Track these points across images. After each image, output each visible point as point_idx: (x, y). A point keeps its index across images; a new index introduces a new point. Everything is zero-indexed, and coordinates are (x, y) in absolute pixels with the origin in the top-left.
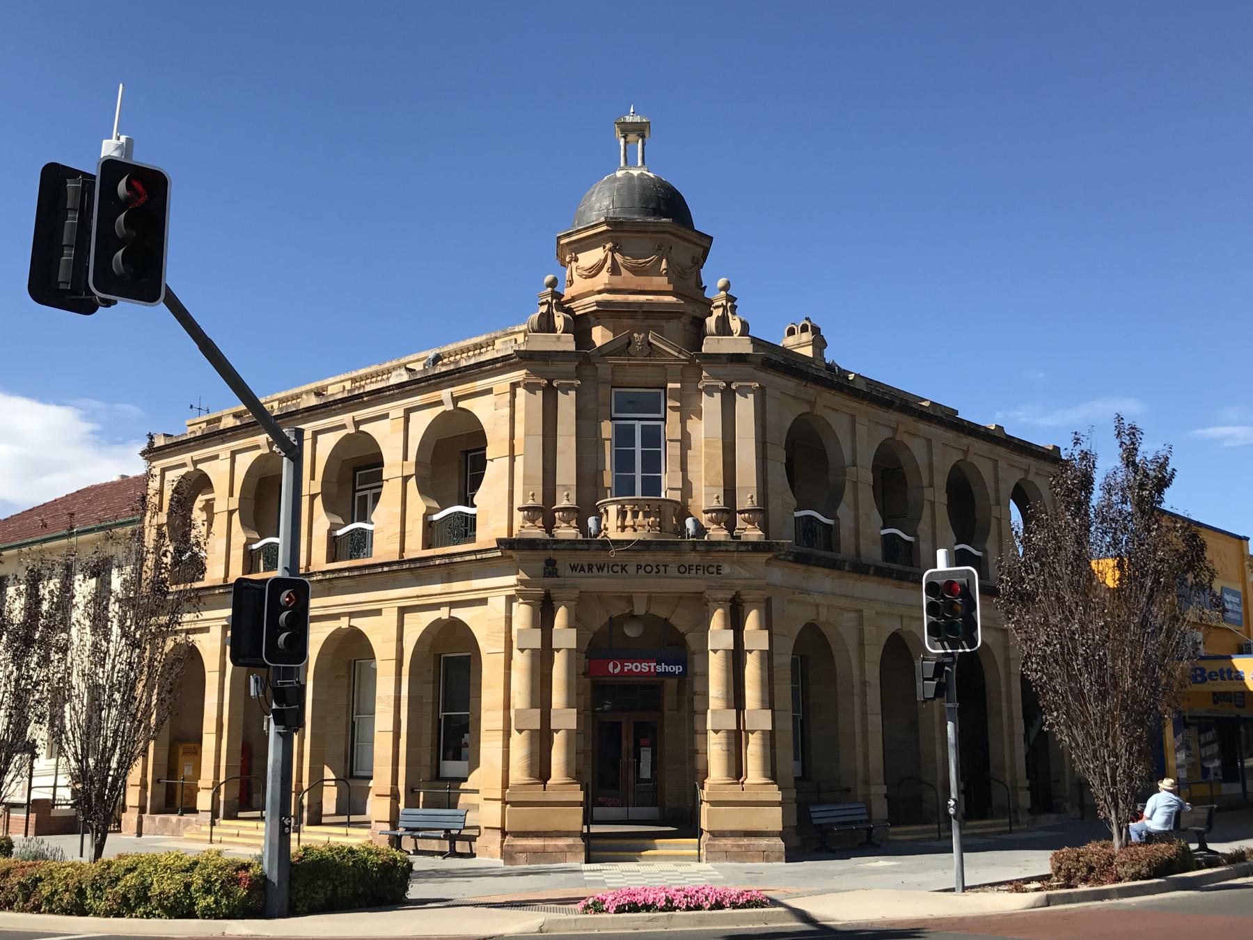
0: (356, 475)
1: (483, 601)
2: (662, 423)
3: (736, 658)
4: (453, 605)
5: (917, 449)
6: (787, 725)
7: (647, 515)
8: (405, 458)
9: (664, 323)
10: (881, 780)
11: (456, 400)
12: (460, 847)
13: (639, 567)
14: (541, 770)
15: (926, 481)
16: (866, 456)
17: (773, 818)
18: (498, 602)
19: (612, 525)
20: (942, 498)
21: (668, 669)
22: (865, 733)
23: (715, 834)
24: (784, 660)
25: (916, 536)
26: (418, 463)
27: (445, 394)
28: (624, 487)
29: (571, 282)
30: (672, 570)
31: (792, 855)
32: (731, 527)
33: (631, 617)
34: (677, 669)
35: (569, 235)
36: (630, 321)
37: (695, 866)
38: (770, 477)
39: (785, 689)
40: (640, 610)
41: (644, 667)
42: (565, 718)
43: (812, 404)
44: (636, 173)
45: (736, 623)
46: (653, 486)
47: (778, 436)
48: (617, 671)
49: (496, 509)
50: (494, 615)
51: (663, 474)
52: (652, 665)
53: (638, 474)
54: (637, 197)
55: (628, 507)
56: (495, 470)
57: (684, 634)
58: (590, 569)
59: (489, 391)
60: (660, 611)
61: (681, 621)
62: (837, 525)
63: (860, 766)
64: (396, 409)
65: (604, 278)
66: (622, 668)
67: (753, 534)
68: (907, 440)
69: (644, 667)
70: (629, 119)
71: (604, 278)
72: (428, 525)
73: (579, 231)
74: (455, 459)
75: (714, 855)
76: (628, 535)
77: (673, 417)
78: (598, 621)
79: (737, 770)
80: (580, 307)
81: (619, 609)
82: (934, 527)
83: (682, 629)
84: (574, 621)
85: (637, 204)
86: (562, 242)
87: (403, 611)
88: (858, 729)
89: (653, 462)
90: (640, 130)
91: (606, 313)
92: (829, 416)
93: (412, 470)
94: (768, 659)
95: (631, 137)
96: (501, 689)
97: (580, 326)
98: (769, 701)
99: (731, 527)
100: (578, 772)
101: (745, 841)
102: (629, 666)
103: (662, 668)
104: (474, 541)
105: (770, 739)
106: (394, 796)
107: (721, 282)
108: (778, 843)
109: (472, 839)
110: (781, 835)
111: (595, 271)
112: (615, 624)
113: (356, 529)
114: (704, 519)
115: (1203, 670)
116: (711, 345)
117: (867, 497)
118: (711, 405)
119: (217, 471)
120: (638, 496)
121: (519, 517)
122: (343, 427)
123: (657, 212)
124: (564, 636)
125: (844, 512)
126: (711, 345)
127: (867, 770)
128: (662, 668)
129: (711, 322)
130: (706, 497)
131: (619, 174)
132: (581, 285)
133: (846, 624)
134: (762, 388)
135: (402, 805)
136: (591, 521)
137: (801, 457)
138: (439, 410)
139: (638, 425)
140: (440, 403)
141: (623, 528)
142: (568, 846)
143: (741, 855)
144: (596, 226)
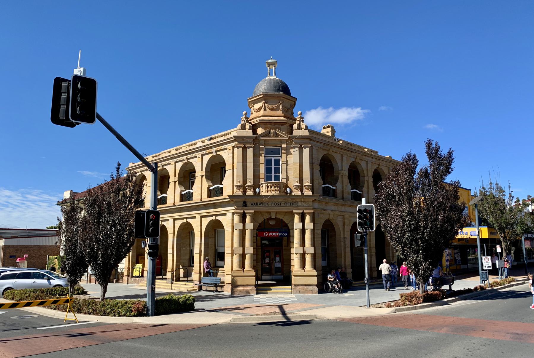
0: (187, 176)
3: (303, 231)
4: (216, 215)
6: (319, 251)
7: (275, 187)
8: (202, 170)
9: (281, 126)
10: (350, 267)
11: (216, 152)
12: (219, 289)
13: (272, 203)
14: (242, 266)
15: (366, 174)
16: (346, 167)
17: (314, 281)
18: (229, 215)
19: (264, 191)
20: (371, 180)
21: (283, 234)
22: (345, 253)
23: (295, 285)
24: (319, 231)
25: (362, 192)
26: (206, 171)
27: (213, 150)
28: (268, 178)
29: (252, 114)
30: (283, 204)
31: (320, 292)
32: (302, 190)
33: (271, 219)
34: (285, 235)
35: (251, 98)
36: (270, 126)
37: (290, 295)
38: (314, 174)
39: (319, 240)
40: (273, 216)
41: (275, 234)
42: (250, 250)
43: (328, 151)
44: (272, 78)
45: (303, 220)
46: (277, 178)
47: (317, 161)
49: (229, 185)
50: (229, 219)
51: (280, 174)
55: (269, 185)
56: (228, 173)
58: (257, 204)
59: (226, 149)
60: (280, 217)
61: (286, 220)
62: (336, 189)
63: (343, 263)
64: (199, 155)
65: (262, 112)
68: (360, 162)
69: (275, 234)
70: (270, 61)
71: (262, 112)
72: (209, 191)
73: (254, 97)
74: (216, 169)
75: (296, 292)
76: (269, 194)
77: (284, 156)
78: (261, 220)
79: (303, 266)
80: (255, 122)
81: (267, 216)
82: (368, 189)
83: (287, 222)
84: (253, 220)
85: (272, 88)
87: (202, 217)
88: (343, 252)
89: (277, 170)
90: (273, 64)
91: (262, 124)
92: (334, 155)
93: (204, 174)
94: (313, 231)
95: (271, 66)
96: (230, 242)
97: (254, 128)
98: (314, 244)
99: (302, 190)
100: (254, 266)
101: (305, 287)
102: (270, 234)
103: (281, 234)
105: (314, 256)
106: (200, 273)
107: (299, 113)
108: (316, 288)
109: (222, 286)
110: (317, 286)
111: (259, 110)
114: (293, 189)
117: (346, 180)
118: (295, 152)
122: (184, 160)
123: (279, 90)
124: (249, 225)
125: (339, 185)
126: (296, 133)
127: (345, 265)
128: (281, 234)
129: (295, 126)
130: (294, 182)
131: (267, 78)
132: (255, 114)
134: (312, 146)
135: (202, 276)
136: (257, 190)
137: (325, 168)
138: (211, 155)
139: (273, 159)
140: (212, 153)
141: (268, 191)
143: (304, 292)
144: (259, 95)
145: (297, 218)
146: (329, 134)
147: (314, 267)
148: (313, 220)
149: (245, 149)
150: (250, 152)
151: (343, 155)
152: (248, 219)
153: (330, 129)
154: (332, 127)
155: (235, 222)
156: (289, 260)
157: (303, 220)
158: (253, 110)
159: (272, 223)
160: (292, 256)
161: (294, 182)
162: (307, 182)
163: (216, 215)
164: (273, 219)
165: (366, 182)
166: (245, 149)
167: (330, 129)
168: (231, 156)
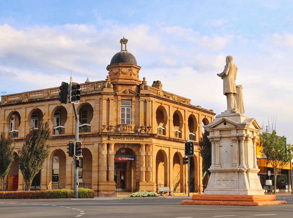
2: (131, 108)
5: (182, 112)
20: (187, 123)
21: (131, 159)
34: (133, 159)
40: (126, 147)
48: (121, 159)
52: (128, 158)
53: (126, 118)
60: (130, 147)
61: (134, 149)
62: (165, 129)
66: (122, 159)
103: (130, 159)
128: (130, 159)
133: (166, 151)
142: (113, 193)
152: (112, 147)
165: (184, 125)
166: (108, 100)
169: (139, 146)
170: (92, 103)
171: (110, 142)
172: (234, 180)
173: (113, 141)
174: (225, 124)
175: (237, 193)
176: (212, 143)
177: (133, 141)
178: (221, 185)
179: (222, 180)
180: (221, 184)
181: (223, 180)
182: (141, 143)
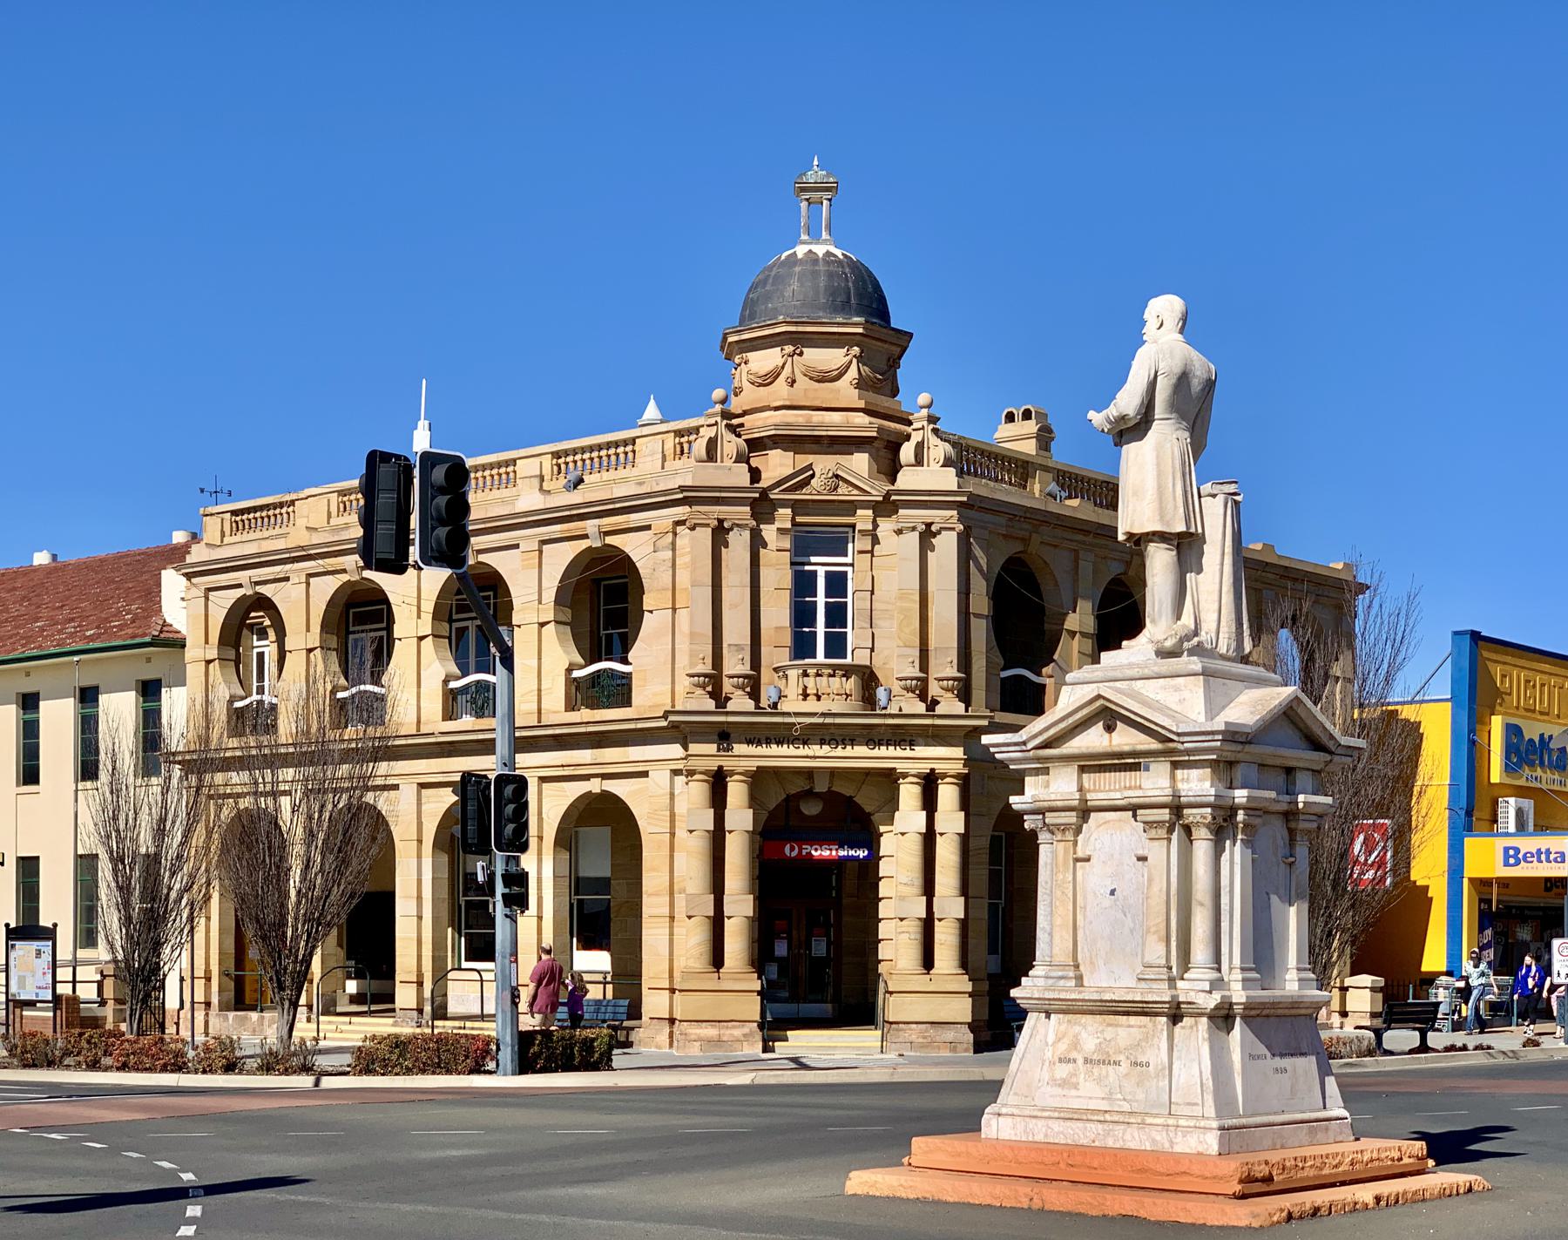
1: (645, 774)
2: (849, 569)
4: (605, 776)
17: (962, 1009)
24: (982, 843)
28: (802, 646)
31: (979, 1048)
33: (809, 794)
39: (981, 874)
40: (821, 787)
42: (740, 905)
43: (1025, 541)
45: (929, 803)
46: (836, 645)
49: (661, 669)
51: (849, 630)
54: (822, 282)
56: (653, 624)
57: (870, 814)
60: (846, 790)
61: (866, 800)
65: (779, 391)
67: (950, 705)
71: (779, 391)
74: (604, 603)
76: (811, 706)
78: (775, 799)
79: (928, 962)
83: (868, 809)
84: (754, 801)
86: (731, 339)
89: (837, 615)
98: (964, 890)
102: (807, 849)
104: (627, 702)
107: (923, 398)
108: (970, 1037)
112: (791, 802)
113: (478, 682)
114: (897, 688)
115: (1517, 850)
116: (907, 479)
119: (287, 598)
120: (820, 657)
121: (684, 683)
123: (844, 307)
124: (740, 817)
129: (907, 452)
130: (896, 665)
131: (801, 250)
132: (750, 396)
139: (821, 571)
141: (805, 696)
145: (909, 794)
146: (1029, 448)
147: (964, 964)
148: (965, 804)
149: (720, 534)
150: (739, 542)
151: (1081, 553)
152: (736, 792)
153: (1031, 427)
154: (1041, 416)
155: (681, 808)
156: (870, 941)
157: (929, 803)
158: (742, 377)
159: (811, 809)
160: (884, 930)
161: (896, 665)
162: (945, 666)
163: (605, 776)
164: (818, 795)
166: (720, 534)
167: (1031, 427)
168: (667, 561)
169: (889, 779)
170: (635, 547)
171: (728, 764)
172: (1148, 1065)
173: (747, 756)
174: (1110, 729)
175: (1154, 1141)
176: (1043, 837)
177: (859, 756)
178: (1076, 1086)
179: (1080, 1061)
180: (1074, 1080)
181: (1086, 1061)
182: (901, 766)
